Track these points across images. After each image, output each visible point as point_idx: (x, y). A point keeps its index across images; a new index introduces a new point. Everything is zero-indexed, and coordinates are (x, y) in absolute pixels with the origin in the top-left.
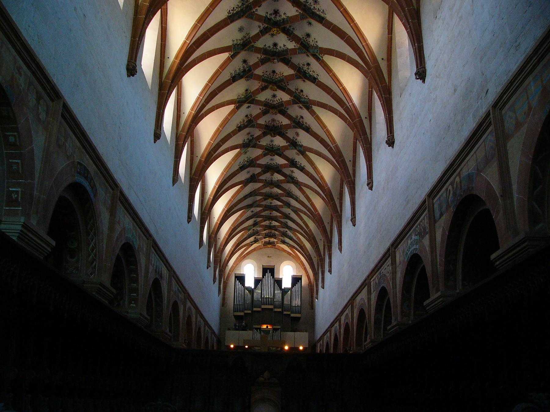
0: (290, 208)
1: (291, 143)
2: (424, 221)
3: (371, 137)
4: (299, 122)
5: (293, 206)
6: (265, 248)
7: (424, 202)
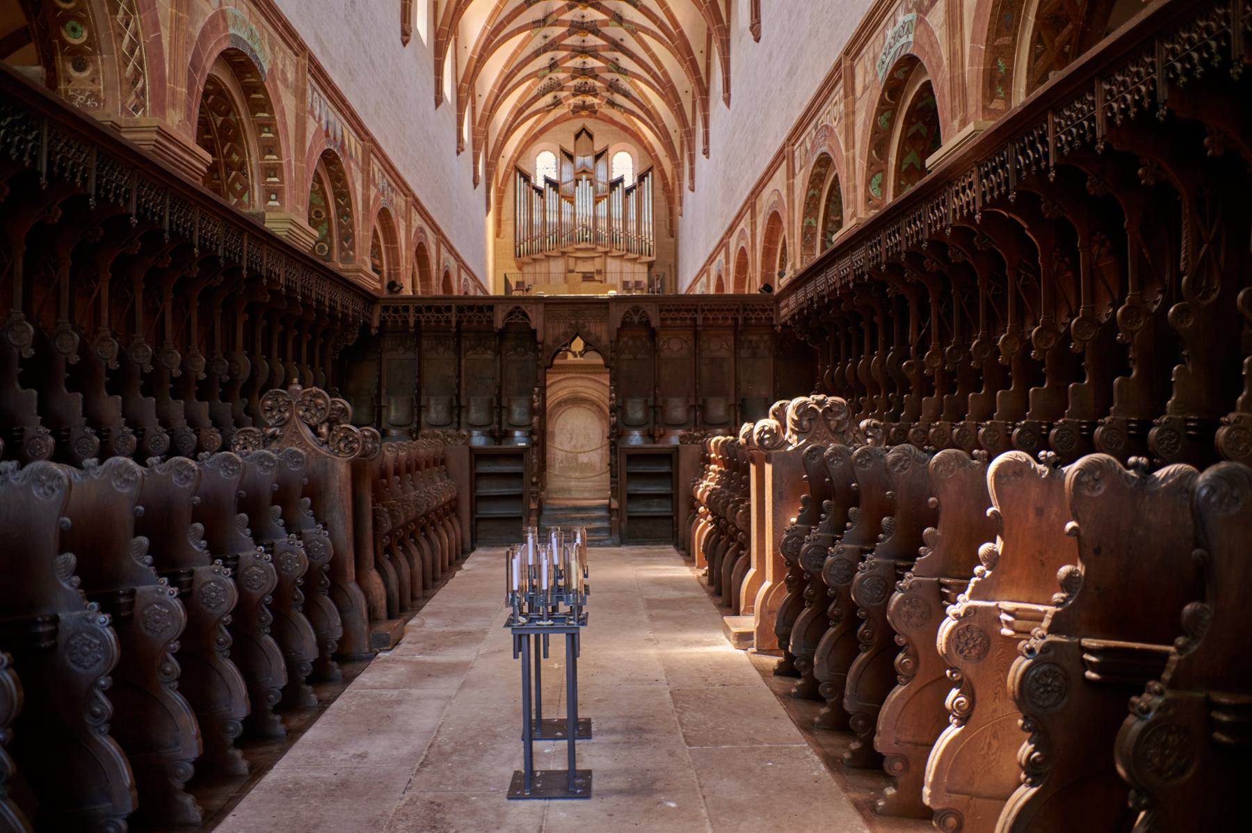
0: (621, 25)
5: (628, 22)
6: (575, 118)
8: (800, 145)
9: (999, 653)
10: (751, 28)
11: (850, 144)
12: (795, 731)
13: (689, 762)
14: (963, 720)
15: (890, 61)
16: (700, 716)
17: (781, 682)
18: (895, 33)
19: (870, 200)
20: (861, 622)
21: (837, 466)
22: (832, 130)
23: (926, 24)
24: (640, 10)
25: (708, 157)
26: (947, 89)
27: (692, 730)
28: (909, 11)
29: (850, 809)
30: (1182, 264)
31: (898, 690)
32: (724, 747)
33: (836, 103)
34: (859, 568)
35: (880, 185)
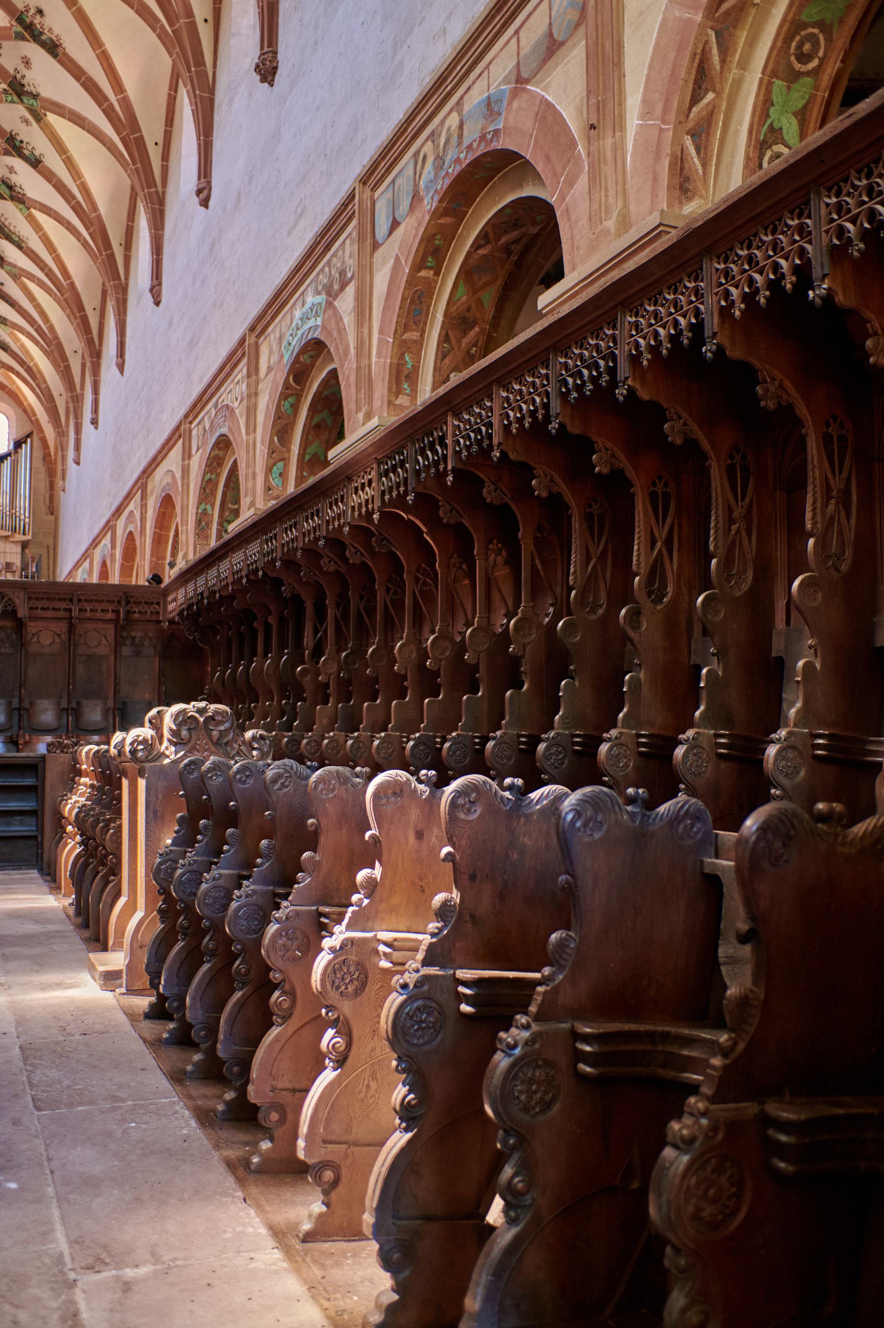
1: (9, 85)
2: (344, 252)
3: (214, 73)
4: (32, 24)
7: (351, 197)
8: (198, 424)
9: (377, 987)
10: (151, 290)
11: (251, 427)
12: (164, 1083)
13: (37, 1131)
14: (341, 1062)
15: (296, 343)
16: (54, 1074)
17: (153, 1026)
18: (304, 314)
19: (269, 489)
20: (236, 956)
21: (216, 782)
22: (233, 411)
23: (335, 309)
24: (24, 253)
25: (96, 428)
26: (353, 379)
27: (43, 1091)
28: (319, 293)
29: (222, 1169)
30: (571, 578)
31: (274, 1032)
32: (79, 1108)
33: (238, 382)
34: (234, 897)
35: (280, 474)
